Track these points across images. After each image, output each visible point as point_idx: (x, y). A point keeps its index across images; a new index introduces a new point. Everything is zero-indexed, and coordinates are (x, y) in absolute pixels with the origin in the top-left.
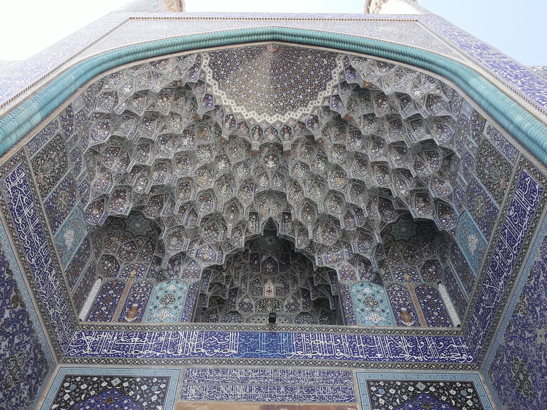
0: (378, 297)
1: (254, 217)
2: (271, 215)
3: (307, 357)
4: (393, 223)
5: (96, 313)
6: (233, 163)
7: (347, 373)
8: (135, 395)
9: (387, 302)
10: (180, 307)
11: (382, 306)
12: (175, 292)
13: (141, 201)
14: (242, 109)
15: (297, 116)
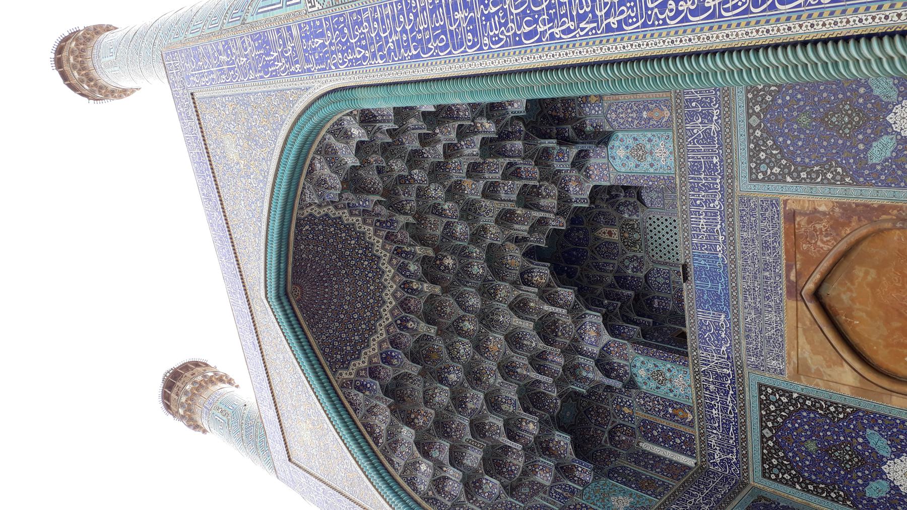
0: (630, 142)
1: (526, 276)
2: (520, 256)
3: (724, 242)
4: (524, 123)
5: (687, 448)
6: (461, 313)
7: (741, 201)
8: (782, 416)
9: (635, 134)
10: (669, 366)
11: (643, 140)
12: (648, 370)
13: (547, 422)
14: (385, 310)
15: (378, 242)
